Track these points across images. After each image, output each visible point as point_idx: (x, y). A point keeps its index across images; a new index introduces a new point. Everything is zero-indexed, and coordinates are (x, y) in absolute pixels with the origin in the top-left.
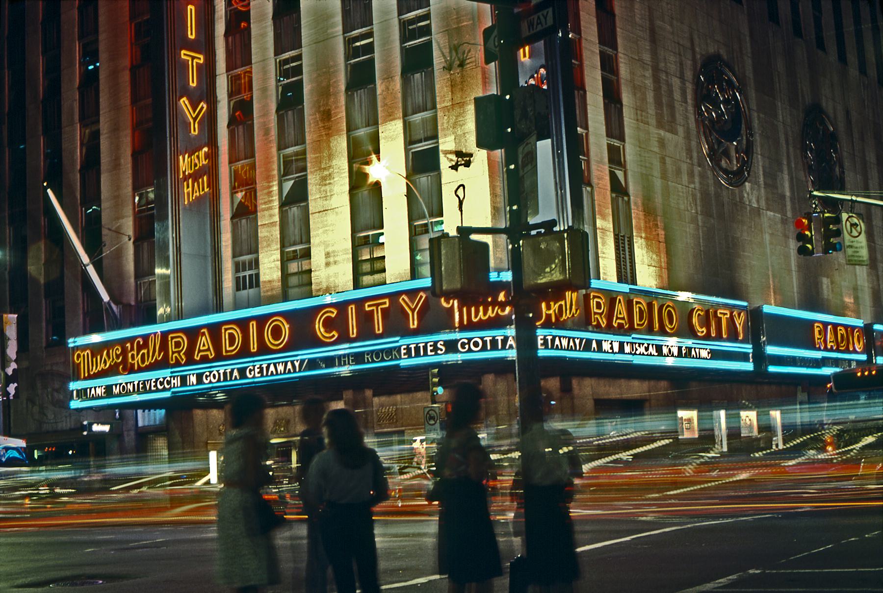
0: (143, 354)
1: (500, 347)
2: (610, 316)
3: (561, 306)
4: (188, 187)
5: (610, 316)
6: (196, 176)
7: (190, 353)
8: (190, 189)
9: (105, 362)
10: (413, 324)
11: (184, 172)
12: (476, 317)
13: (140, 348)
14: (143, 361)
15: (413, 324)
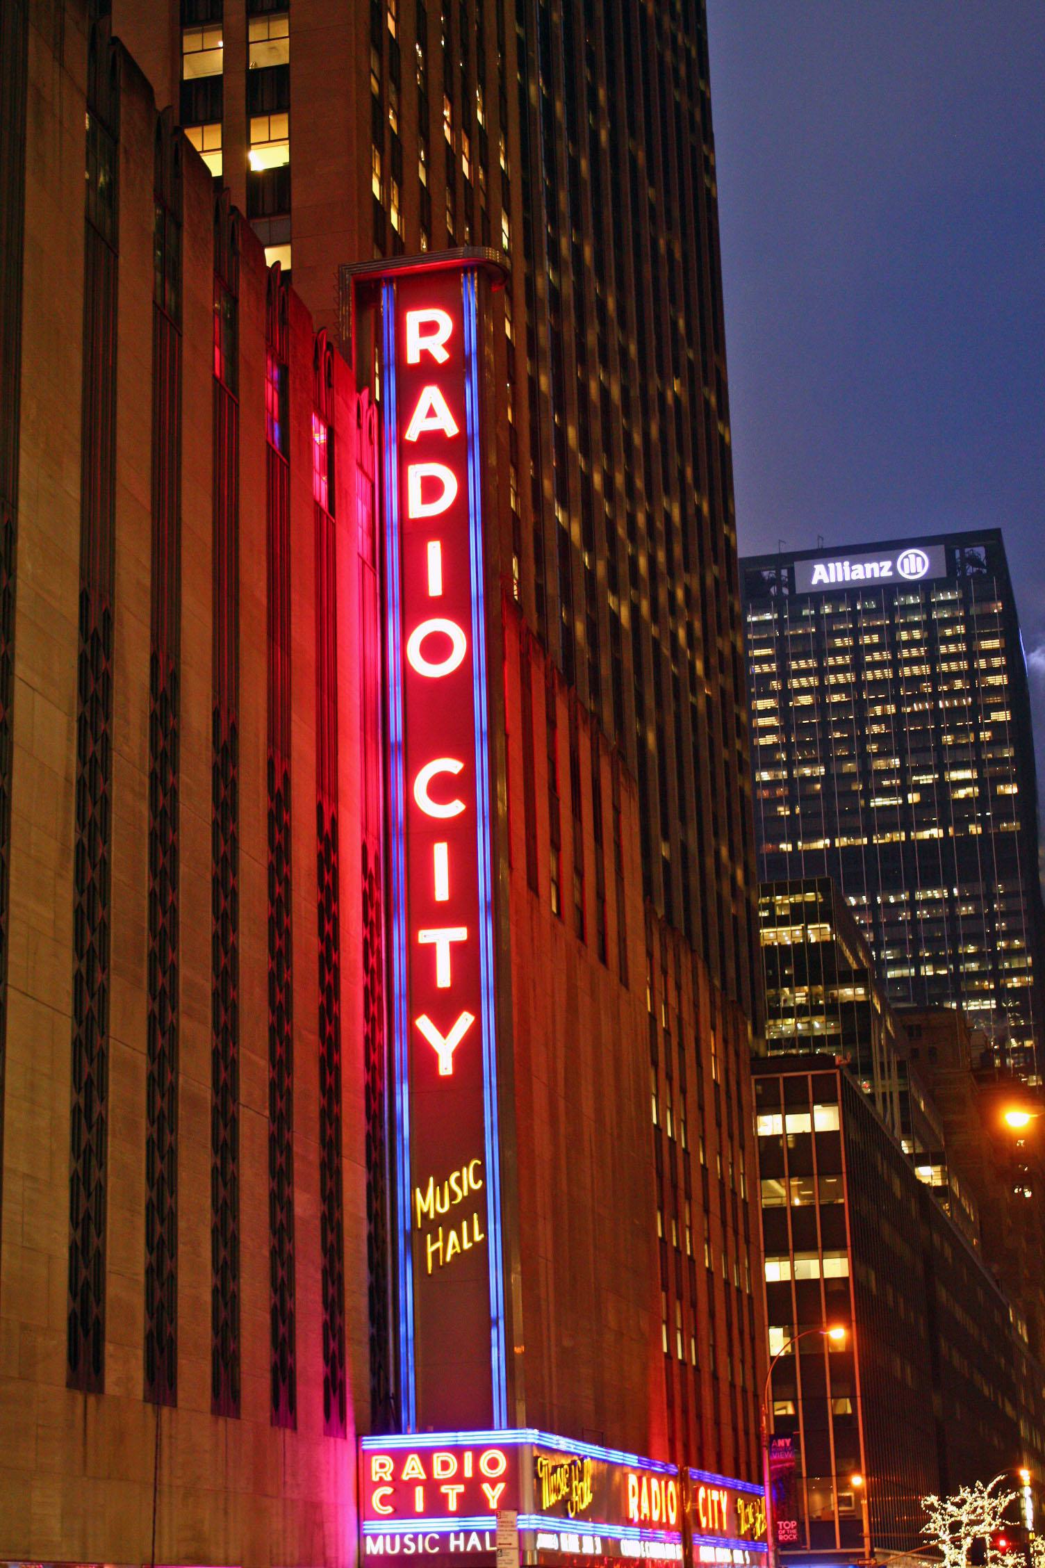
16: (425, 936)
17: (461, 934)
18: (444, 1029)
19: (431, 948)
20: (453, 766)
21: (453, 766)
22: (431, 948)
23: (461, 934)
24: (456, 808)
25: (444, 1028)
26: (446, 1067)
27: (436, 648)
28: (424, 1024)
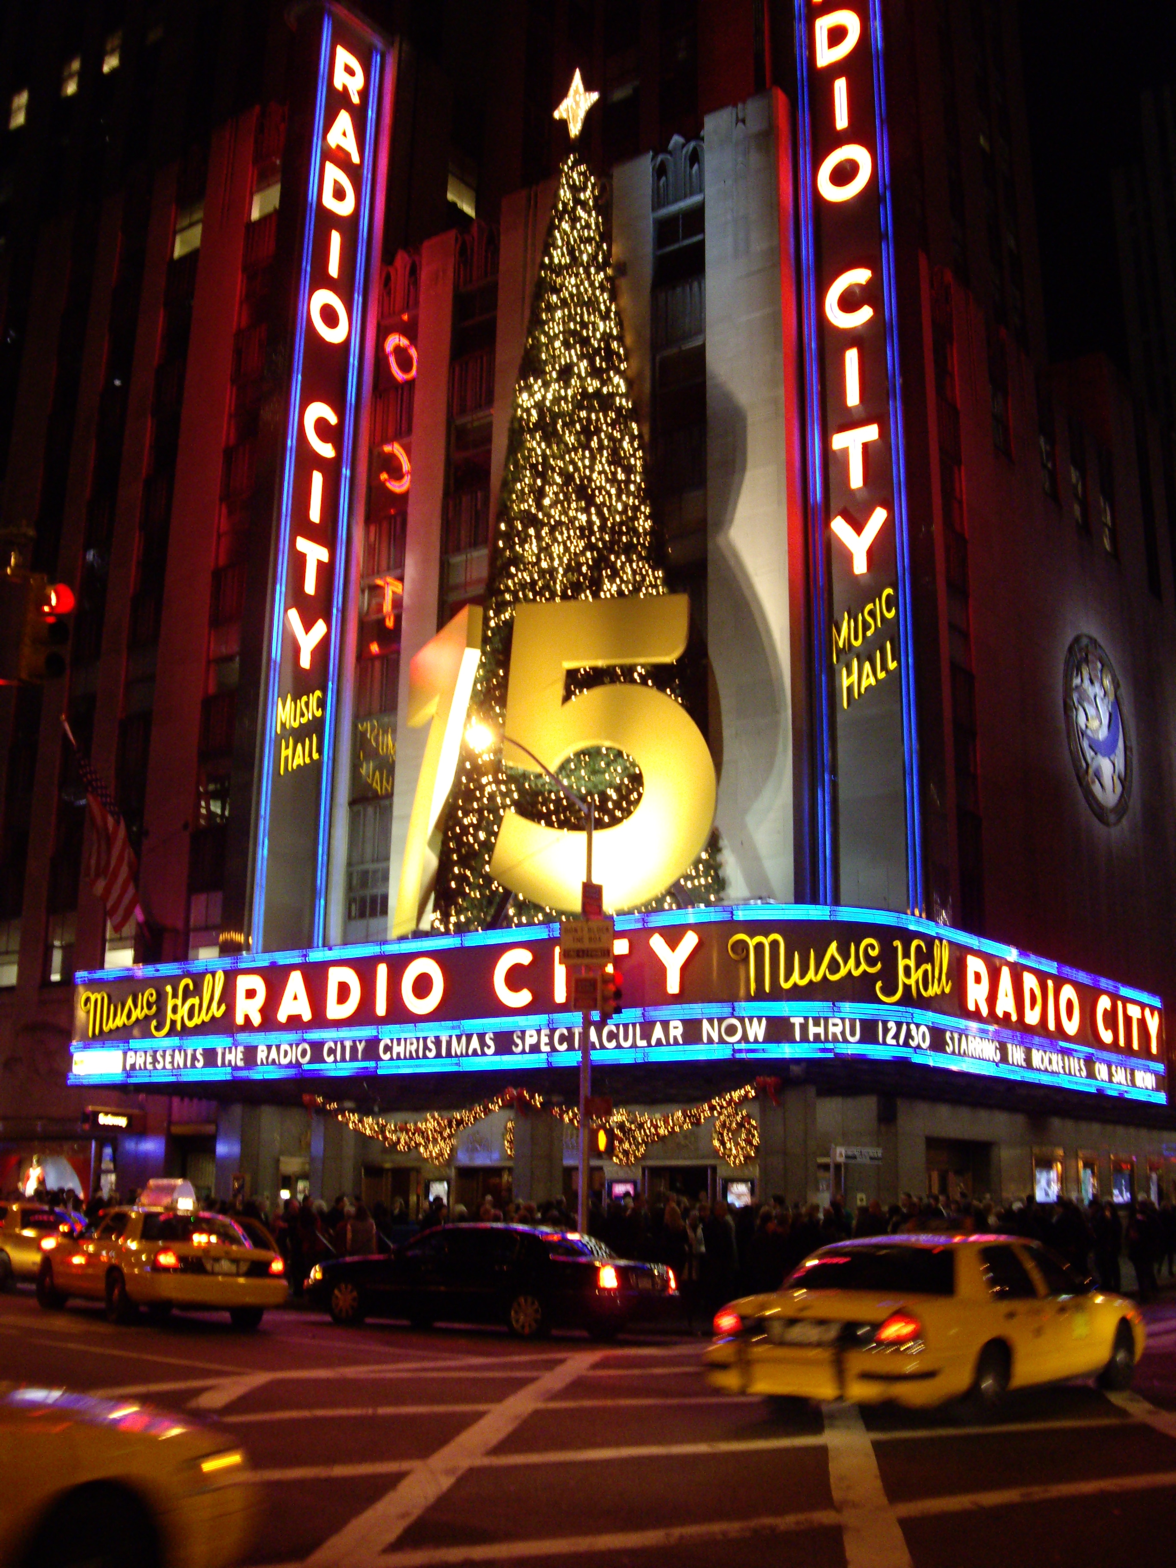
0: (193, 1006)
1: (798, 1038)
2: (992, 999)
3: (926, 973)
4: (287, 747)
5: (992, 999)
6: (300, 734)
7: (269, 1009)
8: (290, 752)
9: (129, 1016)
10: (673, 986)
11: (283, 725)
12: (787, 979)
13: (187, 994)
14: (191, 1016)
15: (673, 986)
16: (839, 441)
17: (871, 433)
18: (858, 528)
19: (845, 452)
20: (860, 276)
21: (860, 276)
22: (845, 452)
23: (871, 433)
24: (865, 313)
25: (858, 528)
26: (860, 566)
27: (844, 174)
28: (839, 526)
